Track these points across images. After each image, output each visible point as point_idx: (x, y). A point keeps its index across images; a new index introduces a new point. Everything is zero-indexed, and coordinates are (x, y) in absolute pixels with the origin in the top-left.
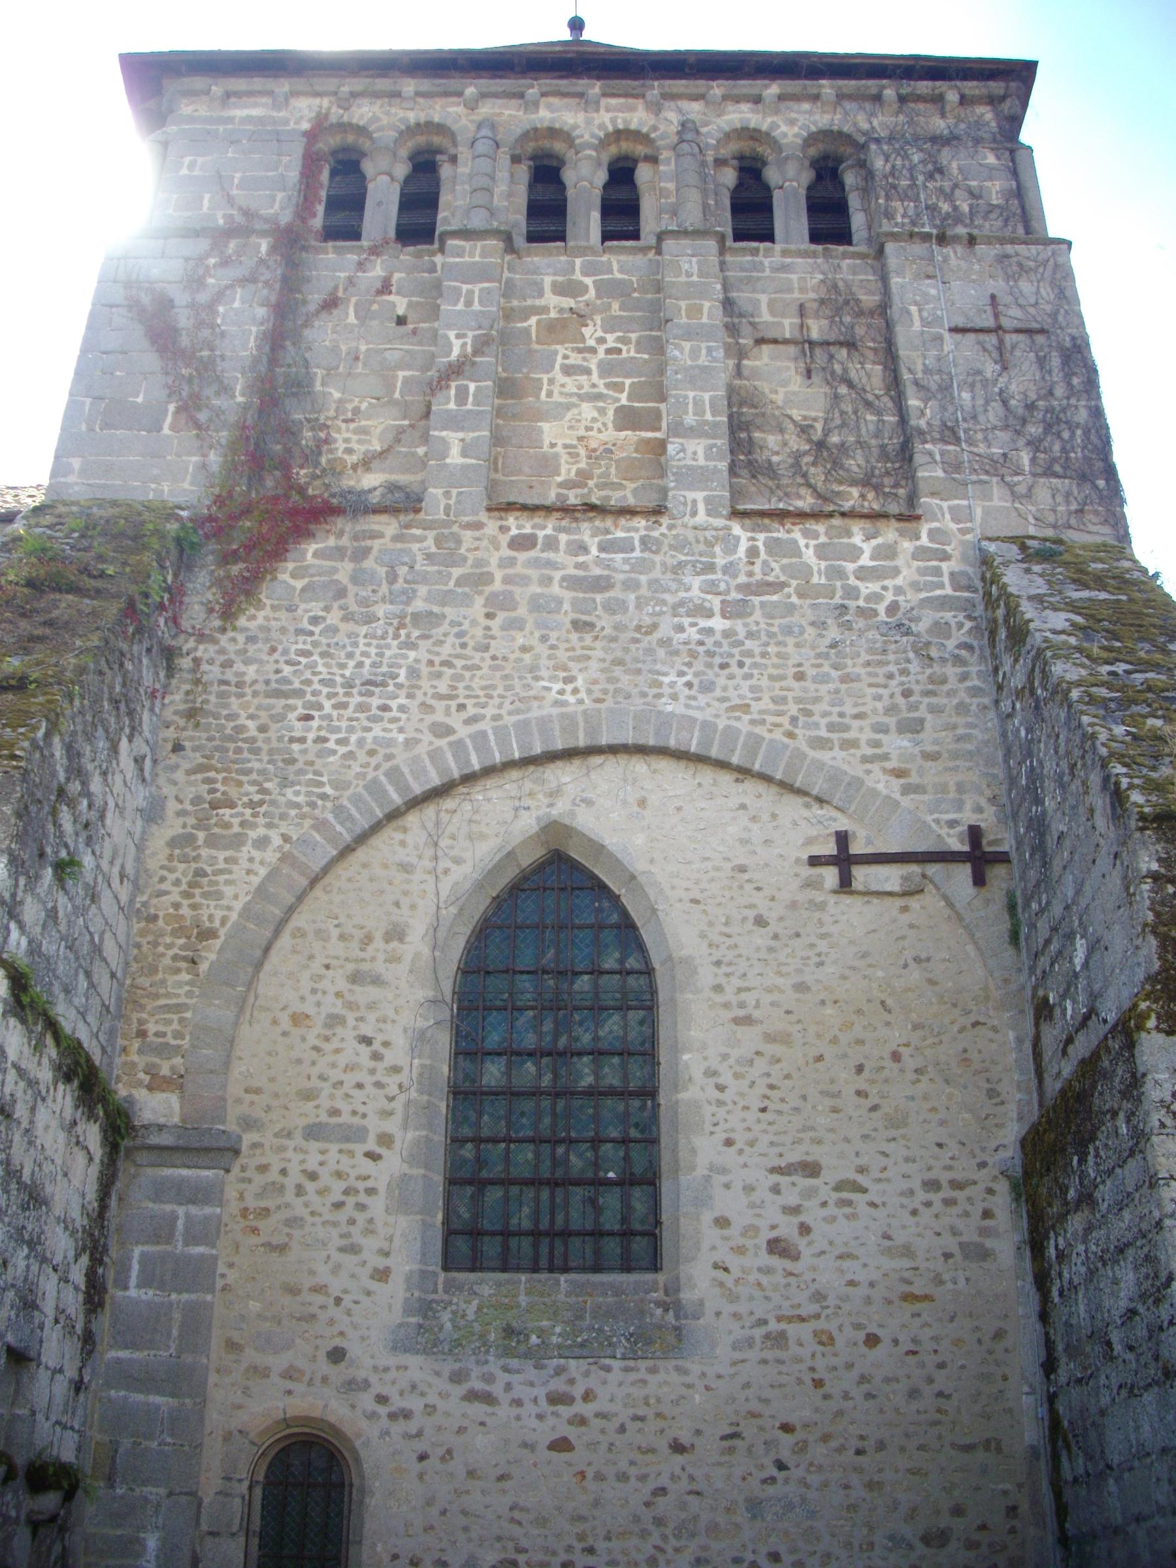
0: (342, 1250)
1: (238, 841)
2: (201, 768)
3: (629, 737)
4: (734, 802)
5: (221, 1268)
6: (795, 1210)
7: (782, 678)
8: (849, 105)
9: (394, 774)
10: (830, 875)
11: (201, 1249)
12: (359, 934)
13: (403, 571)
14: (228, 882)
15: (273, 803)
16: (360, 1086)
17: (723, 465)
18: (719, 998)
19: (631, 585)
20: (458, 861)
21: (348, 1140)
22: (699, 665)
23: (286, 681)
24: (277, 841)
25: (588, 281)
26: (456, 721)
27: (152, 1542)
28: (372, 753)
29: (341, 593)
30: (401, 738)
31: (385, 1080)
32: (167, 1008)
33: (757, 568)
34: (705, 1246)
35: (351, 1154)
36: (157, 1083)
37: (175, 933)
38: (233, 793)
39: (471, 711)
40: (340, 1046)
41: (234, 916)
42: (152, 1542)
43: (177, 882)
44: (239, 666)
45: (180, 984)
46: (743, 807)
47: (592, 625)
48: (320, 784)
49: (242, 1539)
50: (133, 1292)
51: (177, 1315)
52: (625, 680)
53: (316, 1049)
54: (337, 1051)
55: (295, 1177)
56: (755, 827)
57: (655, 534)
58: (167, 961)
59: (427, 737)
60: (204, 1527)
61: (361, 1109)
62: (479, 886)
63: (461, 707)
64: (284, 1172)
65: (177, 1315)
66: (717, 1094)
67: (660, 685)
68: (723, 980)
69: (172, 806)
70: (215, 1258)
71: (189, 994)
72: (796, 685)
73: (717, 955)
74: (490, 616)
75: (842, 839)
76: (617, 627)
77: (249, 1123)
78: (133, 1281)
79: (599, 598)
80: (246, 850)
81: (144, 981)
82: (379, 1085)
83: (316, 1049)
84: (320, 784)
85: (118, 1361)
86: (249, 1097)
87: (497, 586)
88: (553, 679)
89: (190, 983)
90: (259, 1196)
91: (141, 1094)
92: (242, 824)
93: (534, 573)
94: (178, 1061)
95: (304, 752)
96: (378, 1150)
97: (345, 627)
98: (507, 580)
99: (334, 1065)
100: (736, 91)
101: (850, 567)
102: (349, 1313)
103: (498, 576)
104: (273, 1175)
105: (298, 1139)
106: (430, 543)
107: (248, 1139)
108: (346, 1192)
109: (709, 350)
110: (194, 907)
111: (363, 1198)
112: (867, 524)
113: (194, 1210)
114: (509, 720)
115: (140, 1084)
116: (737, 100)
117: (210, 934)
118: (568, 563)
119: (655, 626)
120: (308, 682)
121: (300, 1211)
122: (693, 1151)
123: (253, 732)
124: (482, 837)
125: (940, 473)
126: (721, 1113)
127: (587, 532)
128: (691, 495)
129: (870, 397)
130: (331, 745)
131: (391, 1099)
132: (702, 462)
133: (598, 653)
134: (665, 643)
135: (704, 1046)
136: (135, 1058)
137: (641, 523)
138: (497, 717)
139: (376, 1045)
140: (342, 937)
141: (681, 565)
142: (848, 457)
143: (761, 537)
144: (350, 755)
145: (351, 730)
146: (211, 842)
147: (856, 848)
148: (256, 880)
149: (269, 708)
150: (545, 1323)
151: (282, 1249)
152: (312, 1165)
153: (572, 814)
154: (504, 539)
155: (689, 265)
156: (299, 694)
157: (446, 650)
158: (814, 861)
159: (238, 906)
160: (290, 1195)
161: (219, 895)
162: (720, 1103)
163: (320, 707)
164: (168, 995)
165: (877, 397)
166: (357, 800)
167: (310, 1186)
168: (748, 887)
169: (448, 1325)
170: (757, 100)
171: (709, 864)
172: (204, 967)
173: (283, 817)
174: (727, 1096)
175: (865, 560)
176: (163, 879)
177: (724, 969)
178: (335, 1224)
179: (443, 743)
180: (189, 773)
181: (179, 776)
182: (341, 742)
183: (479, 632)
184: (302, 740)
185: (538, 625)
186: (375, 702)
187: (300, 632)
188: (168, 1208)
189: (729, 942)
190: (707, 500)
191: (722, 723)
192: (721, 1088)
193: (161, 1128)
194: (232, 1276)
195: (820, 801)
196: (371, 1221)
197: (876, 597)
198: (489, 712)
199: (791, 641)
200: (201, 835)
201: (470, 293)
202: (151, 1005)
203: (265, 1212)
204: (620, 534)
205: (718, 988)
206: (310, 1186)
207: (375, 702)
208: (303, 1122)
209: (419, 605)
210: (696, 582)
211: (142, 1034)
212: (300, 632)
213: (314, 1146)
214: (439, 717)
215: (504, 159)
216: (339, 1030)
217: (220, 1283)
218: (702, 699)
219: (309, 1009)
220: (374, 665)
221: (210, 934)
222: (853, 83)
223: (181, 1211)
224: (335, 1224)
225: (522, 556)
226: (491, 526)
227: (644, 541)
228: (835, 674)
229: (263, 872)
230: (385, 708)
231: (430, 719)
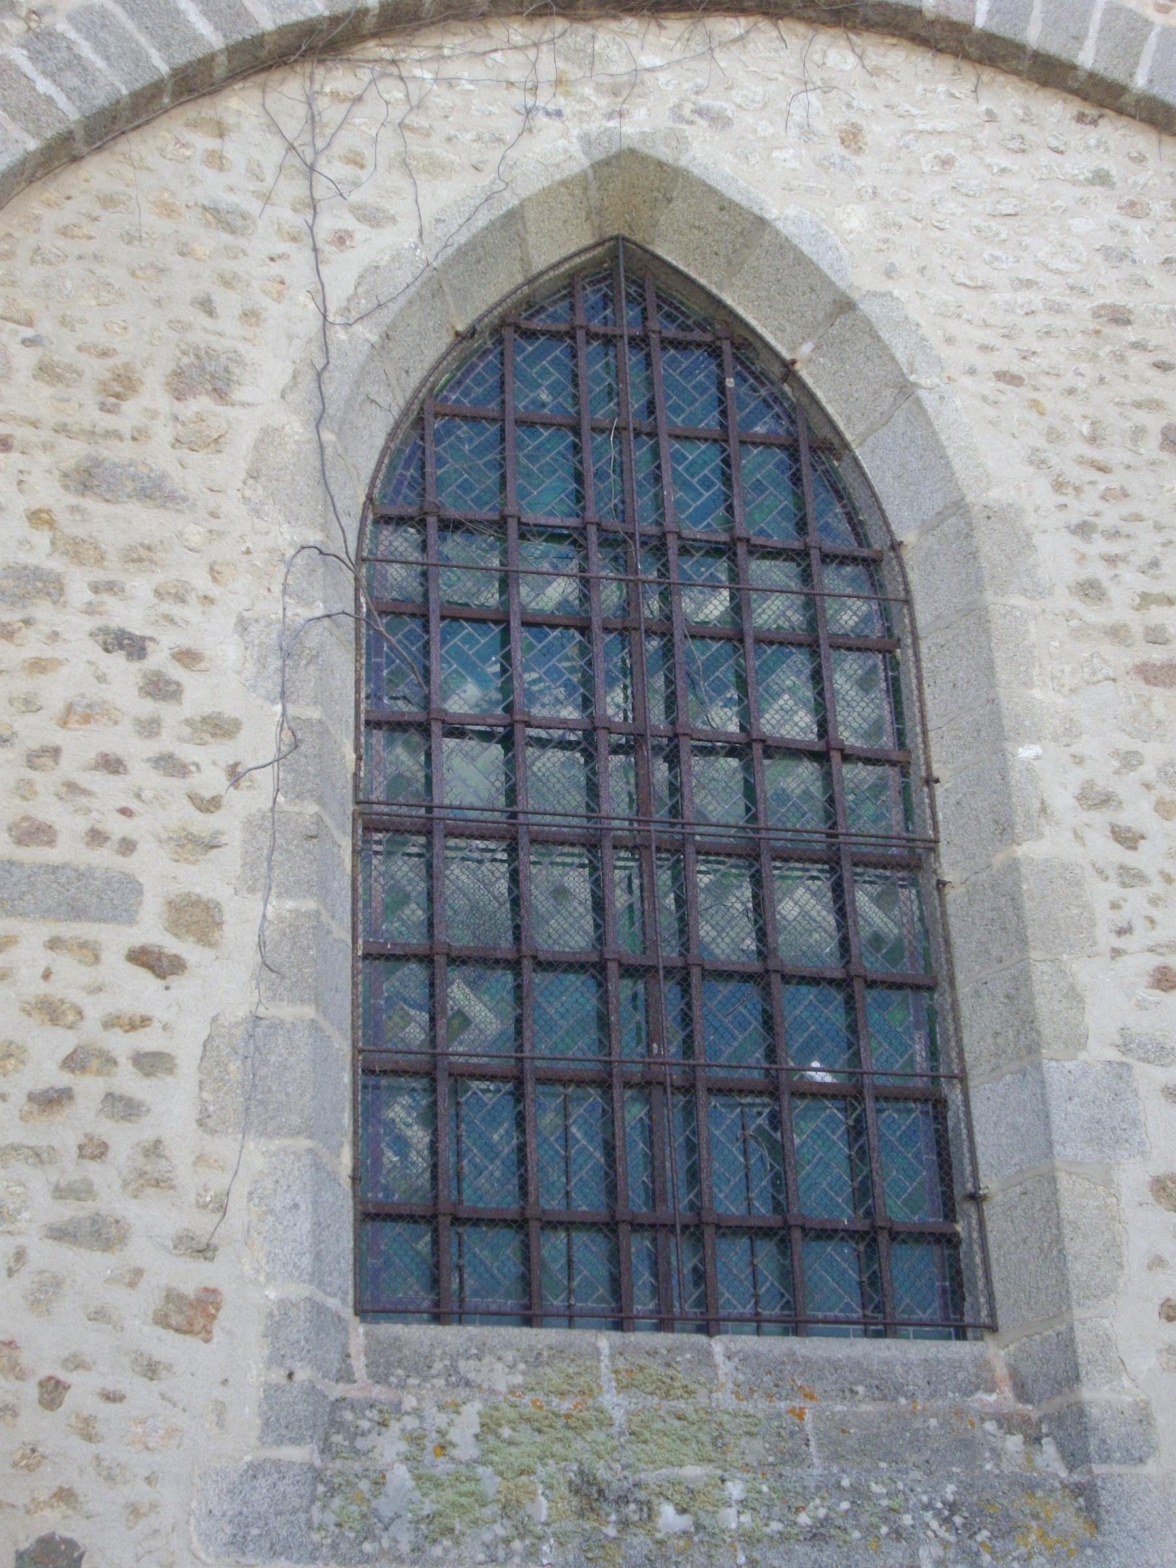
0: (61, 1234)
4: (1080, 164)
12: (96, 369)
16: (111, 765)
18: (1093, 615)
20: (373, 217)
21: (77, 912)
31: (188, 753)
34: (1136, 1252)
35: (90, 952)
40: (47, 653)
46: (1101, 178)
56: (1137, 227)
61: (118, 828)
66: (1118, 854)
68: (1100, 571)
73: (1080, 510)
82: (168, 764)
96: (172, 945)
99: (29, 704)
102: (87, 1430)
108: (74, 1062)
111: (127, 1081)
122: (1074, 996)
124: (437, 168)
126: (1136, 901)
131: (211, 805)
135: (1071, 730)
139: (158, 659)
140: (46, 371)
150: (692, 1471)
153: (681, 142)
162: (1130, 877)
168: (1138, 361)
169: (400, 1474)
171: (1035, 299)
174: (1142, 859)
177: (1100, 545)
178: (38, 1156)
189: (1104, 482)
192: (1127, 838)
196: (155, 1149)
205: (1090, 590)
216: (42, 610)
224: (38, 1156)
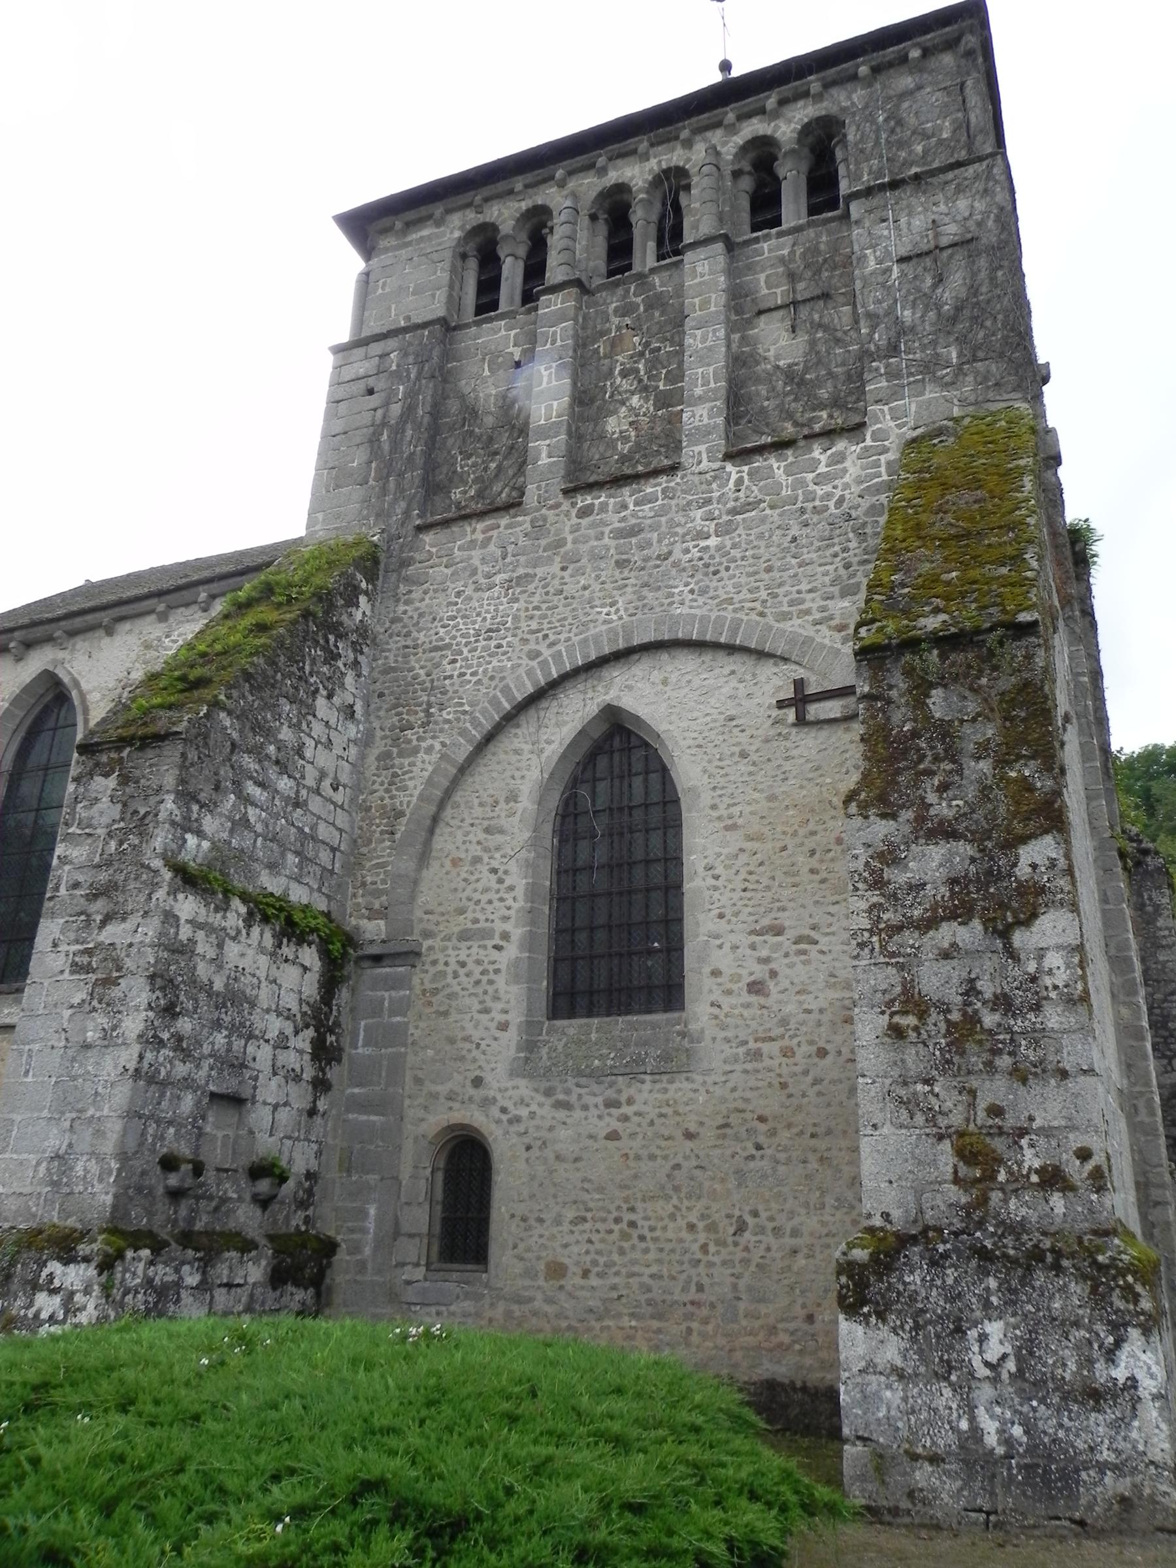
0: (480, 1012)
1: (416, 751)
2: (396, 706)
3: (650, 636)
4: (726, 671)
5: (412, 1030)
6: (766, 961)
7: (756, 573)
8: (834, 91)
9: (506, 690)
10: (791, 715)
11: (398, 1019)
12: (490, 800)
13: (510, 548)
14: (411, 779)
15: (436, 723)
16: (490, 902)
17: (720, 420)
18: (715, 814)
19: (653, 528)
20: (549, 742)
21: (483, 938)
22: (699, 576)
23: (442, 639)
24: (438, 747)
25: (639, 300)
26: (542, 648)
27: (372, 1211)
28: (492, 678)
29: (474, 572)
30: (509, 664)
31: (505, 896)
32: (378, 866)
33: (741, 494)
35: (485, 947)
36: (373, 914)
37: (381, 817)
38: (412, 719)
39: (552, 638)
41: (415, 799)
42: (372, 1211)
43: (382, 784)
44: (415, 634)
45: (384, 850)
46: (733, 672)
47: (629, 561)
48: (462, 704)
49: (427, 1207)
50: (360, 1051)
51: (385, 1063)
52: (650, 595)
53: (465, 880)
54: (478, 880)
55: (453, 966)
56: (741, 686)
57: (672, 484)
58: (377, 835)
59: (525, 661)
60: (403, 1200)
61: (491, 917)
62: (564, 757)
63: (546, 636)
64: (446, 964)
65: (385, 1063)
66: (713, 882)
67: (672, 595)
68: (717, 801)
69: (379, 733)
70: (407, 1024)
71: (389, 855)
72: (766, 576)
73: (714, 782)
74: (563, 569)
75: (799, 684)
76: (646, 559)
77: (427, 934)
78: (360, 1043)
79: (634, 540)
80: (421, 755)
81: (364, 850)
82: (502, 900)
83: (465, 880)
84: (462, 704)
85: (353, 1095)
86: (426, 917)
87: (569, 546)
88: (603, 606)
89: (390, 848)
90: (433, 980)
91: (364, 923)
92: (418, 739)
93: (591, 532)
94: (384, 898)
95: (452, 685)
96: (501, 943)
97: (476, 595)
98: (575, 542)
99: (475, 891)
100: (746, 109)
101: (811, 476)
102: (484, 1053)
103: (570, 538)
104: (440, 967)
105: (454, 941)
106: (528, 526)
107: (426, 944)
108: (482, 973)
109: (714, 331)
110: (391, 798)
111: (492, 976)
112: (826, 442)
113: (393, 993)
114: (576, 639)
115: (362, 917)
116: (748, 116)
117: (401, 814)
118: (614, 520)
119: (670, 553)
120: (454, 638)
121: (457, 989)
122: (697, 923)
123: (423, 677)
124: (565, 723)
125: (885, 384)
126: (716, 895)
127: (626, 494)
128: (697, 449)
129: (839, 334)
130: (468, 677)
131: (509, 908)
132: (706, 421)
133: (632, 581)
134: (675, 564)
135: (705, 848)
136: (360, 900)
137: (663, 479)
138: (568, 639)
139: (500, 873)
140: (481, 805)
141: (689, 503)
142: (820, 388)
143: (746, 468)
144: (479, 682)
145: (479, 665)
146: (401, 754)
147: (811, 690)
148: (426, 774)
149: (432, 659)
150: (605, 1051)
151: (446, 1014)
152: (463, 958)
153: (619, 697)
154: (574, 512)
155: (703, 267)
156: (448, 646)
157: (536, 599)
158: (781, 704)
159: (417, 793)
160: (449, 979)
161: (405, 788)
162: (716, 888)
163: (461, 653)
164: (379, 857)
165: (845, 333)
166: (484, 712)
167: (462, 971)
168: (736, 731)
169: (545, 1057)
170: (762, 111)
171: (709, 718)
172: (398, 836)
173: (441, 731)
175: (822, 469)
176: (374, 782)
177: (719, 792)
178: (475, 995)
179: (534, 663)
180: (388, 710)
181: (382, 713)
182: (473, 674)
183: (556, 582)
184: (451, 677)
185: (594, 569)
186: (493, 643)
187: (450, 604)
188: (379, 993)
189: (722, 772)
190: (709, 451)
191: (713, 616)
192: (717, 877)
193: (372, 942)
194: (417, 1033)
195: (785, 660)
196: (496, 991)
197: (828, 496)
198: (562, 637)
199: (762, 543)
200: (395, 750)
201: (555, 333)
202: (368, 865)
203: (435, 992)
204: (649, 490)
205: (714, 807)
206: (462, 971)
207: (493, 643)
208: (456, 930)
209: (521, 571)
210: (698, 514)
211: (364, 884)
212: (450, 604)
213: (464, 944)
214: (532, 646)
215: (584, 221)
216: (478, 866)
217: (410, 1040)
218: (701, 600)
219: (463, 856)
220: (493, 618)
221: (401, 814)
222: (833, 70)
223: (386, 994)
224: (475, 995)
225: (585, 522)
226: (566, 505)
227: (664, 491)
228: (794, 561)
229: (430, 768)
230: (499, 646)
231: (526, 648)
